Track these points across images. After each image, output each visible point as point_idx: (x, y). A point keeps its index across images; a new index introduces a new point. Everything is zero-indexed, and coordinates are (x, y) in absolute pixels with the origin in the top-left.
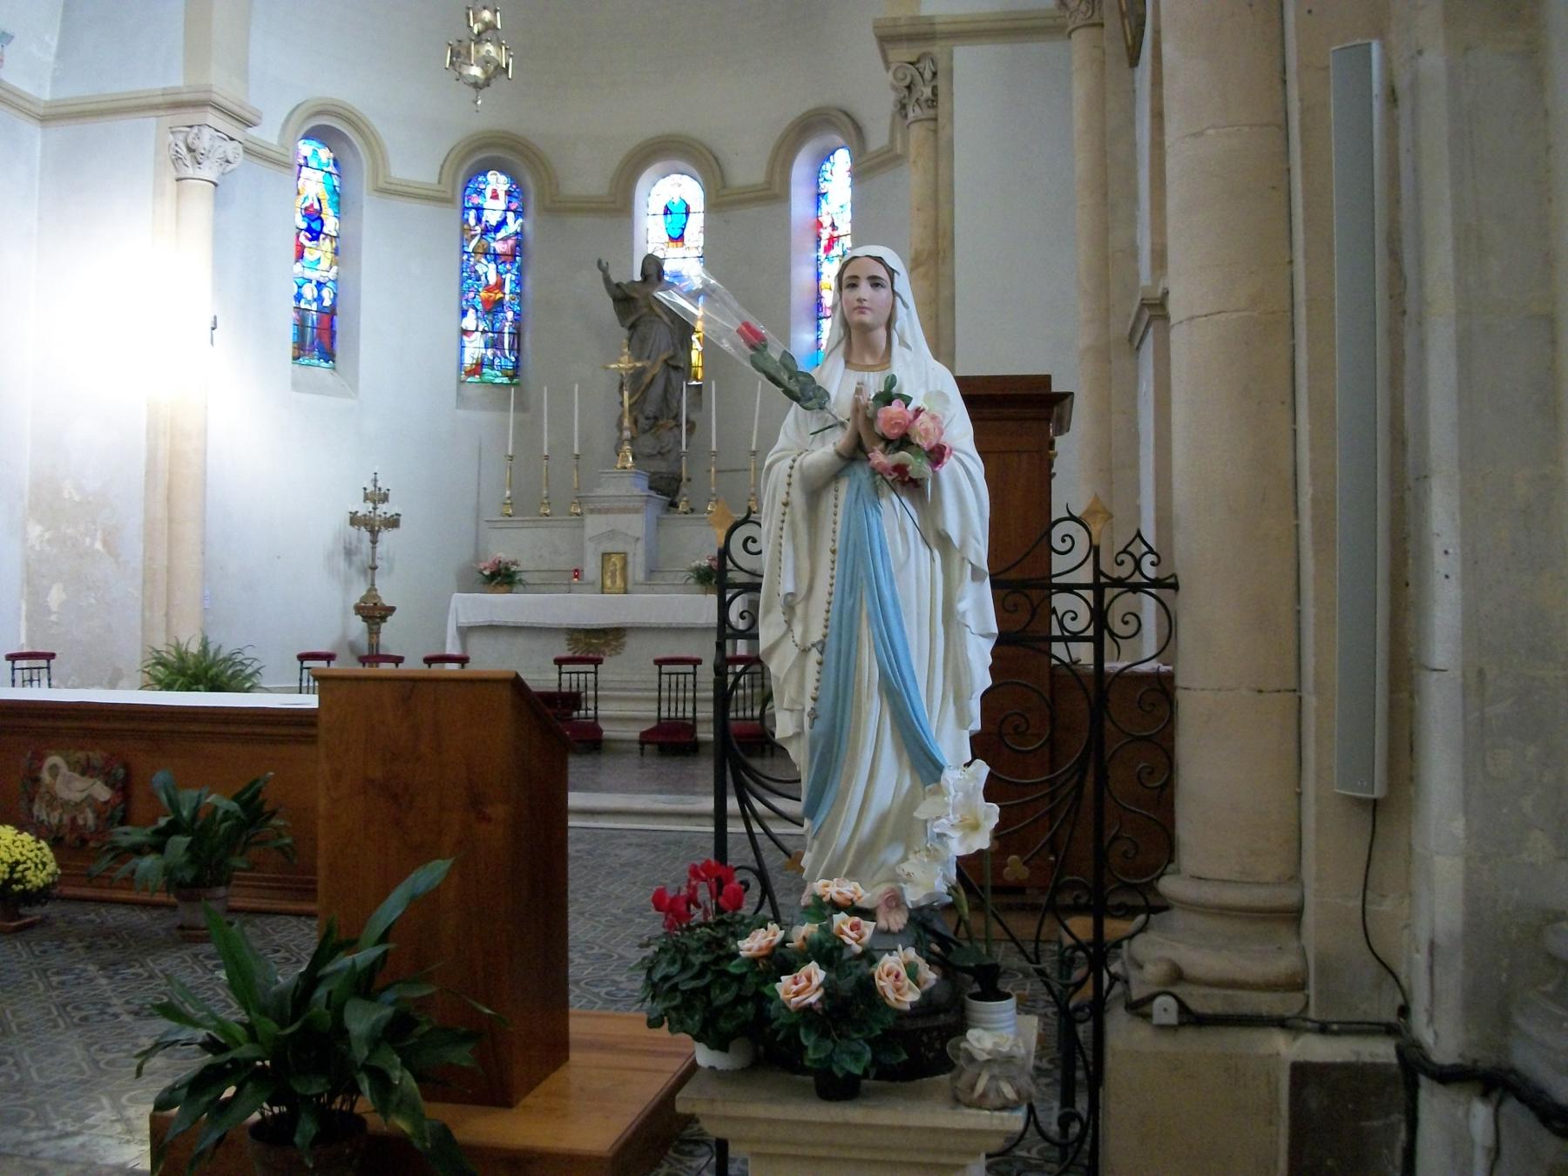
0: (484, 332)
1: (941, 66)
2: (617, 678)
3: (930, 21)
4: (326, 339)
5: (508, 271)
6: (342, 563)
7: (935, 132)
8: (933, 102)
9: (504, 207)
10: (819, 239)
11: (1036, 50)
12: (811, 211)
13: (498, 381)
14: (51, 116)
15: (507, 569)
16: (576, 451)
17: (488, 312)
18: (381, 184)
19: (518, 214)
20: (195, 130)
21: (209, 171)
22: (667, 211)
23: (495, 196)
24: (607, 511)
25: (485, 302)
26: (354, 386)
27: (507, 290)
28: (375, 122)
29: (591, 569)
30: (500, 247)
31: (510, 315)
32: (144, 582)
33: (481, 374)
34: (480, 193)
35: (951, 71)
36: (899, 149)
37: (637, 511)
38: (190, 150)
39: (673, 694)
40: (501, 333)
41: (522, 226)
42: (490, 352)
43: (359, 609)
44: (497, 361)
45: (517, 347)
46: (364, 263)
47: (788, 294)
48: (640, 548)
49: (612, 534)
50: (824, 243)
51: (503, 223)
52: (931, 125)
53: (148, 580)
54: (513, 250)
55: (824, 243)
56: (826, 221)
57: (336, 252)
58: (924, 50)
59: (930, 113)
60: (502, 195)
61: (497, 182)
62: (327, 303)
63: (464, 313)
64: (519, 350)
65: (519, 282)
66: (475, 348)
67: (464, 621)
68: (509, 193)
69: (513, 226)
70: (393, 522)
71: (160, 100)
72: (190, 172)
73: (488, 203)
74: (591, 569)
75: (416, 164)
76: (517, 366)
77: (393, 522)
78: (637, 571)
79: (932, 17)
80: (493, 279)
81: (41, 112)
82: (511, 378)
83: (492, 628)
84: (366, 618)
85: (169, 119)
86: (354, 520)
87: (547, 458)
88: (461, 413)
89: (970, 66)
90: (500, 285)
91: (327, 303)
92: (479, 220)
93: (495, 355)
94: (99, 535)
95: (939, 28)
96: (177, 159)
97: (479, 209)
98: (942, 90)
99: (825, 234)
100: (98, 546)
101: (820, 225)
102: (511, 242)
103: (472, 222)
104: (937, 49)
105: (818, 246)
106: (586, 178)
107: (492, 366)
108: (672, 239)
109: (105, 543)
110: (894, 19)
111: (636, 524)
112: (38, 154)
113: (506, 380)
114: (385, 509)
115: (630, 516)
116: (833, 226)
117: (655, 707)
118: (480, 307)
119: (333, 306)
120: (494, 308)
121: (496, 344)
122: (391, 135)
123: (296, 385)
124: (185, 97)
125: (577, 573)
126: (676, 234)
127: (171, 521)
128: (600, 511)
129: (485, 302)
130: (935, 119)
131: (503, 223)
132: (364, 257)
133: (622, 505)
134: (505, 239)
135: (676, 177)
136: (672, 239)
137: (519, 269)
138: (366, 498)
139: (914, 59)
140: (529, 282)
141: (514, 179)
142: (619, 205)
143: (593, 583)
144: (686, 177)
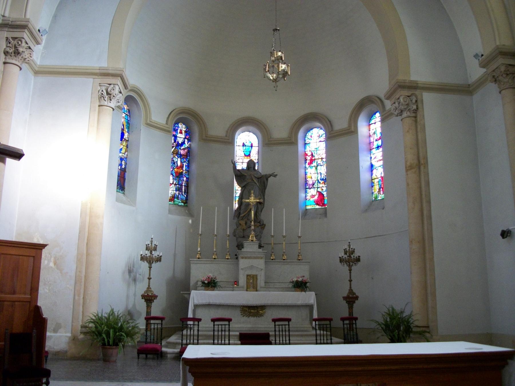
0: (175, 184)
1: (419, 97)
2: (263, 326)
3: (416, 82)
4: (122, 180)
5: (185, 162)
6: (127, 276)
7: (416, 121)
8: (416, 111)
9: (184, 137)
10: (306, 160)
11: (450, 97)
12: (303, 149)
13: (180, 204)
14: (39, 72)
15: (214, 281)
16: (200, 233)
17: (177, 177)
18: (148, 122)
19: (189, 140)
20: (112, 86)
21: (113, 104)
22: (244, 145)
23: (181, 133)
24: (249, 258)
25: (176, 173)
26: (132, 202)
27: (184, 169)
28: (147, 97)
29: (242, 281)
30: (182, 152)
31: (185, 179)
32: (75, 283)
33: (174, 201)
34: (176, 130)
35: (422, 101)
36: (353, 129)
37: (262, 258)
38: (108, 93)
39: (284, 333)
40: (182, 185)
41: (190, 145)
42: (177, 193)
43: (143, 297)
44: (180, 196)
45: (187, 192)
46: (140, 152)
47: (298, 177)
48: (263, 273)
49: (252, 267)
50: (308, 161)
51: (183, 143)
52: (414, 119)
53: (77, 281)
54: (187, 153)
55: (308, 161)
56: (309, 154)
57: (127, 147)
58: (412, 92)
59: (414, 115)
60: (183, 132)
61: (182, 127)
62: (123, 167)
64: (188, 193)
65: (188, 166)
66: (172, 190)
67: (196, 302)
68: (185, 132)
69: (186, 145)
70: (159, 259)
71: (98, 71)
72: (106, 103)
73: (179, 135)
74: (242, 281)
75: (159, 116)
76: (187, 199)
77: (159, 259)
78: (261, 282)
79: (417, 81)
80: (179, 164)
81: (37, 69)
82: (185, 203)
83: (209, 306)
84: (146, 300)
85: (99, 80)
86: (143, 258)
87: (216, 236)
88: (169, 215)
89: (428, 99)
90: (182, 167)
91: (123, 167)
92: (175, 141)
93: (179, 194)
94: (52, 259)
95: (420, 85)
96: (101, 97)
97: (175, 137)
98: (420, 106)
99: (309, 158)
100: (52, 264)
101: (306, 155)
102: (186, 151)
104: (417, 92)
105: (306, 163)
106: (217, 130)
107: (178, 198)
108: (245, 155)
109: (55, 264)
110: (404, 80)
111: (260, 263)
112: (32, 87)
113: (182, 204)
114: (155, 254)
115: (259, 260)
116: (312, 155)
117: (315, 339)
118: (174, 175)
119: (125, 168)
120: (178, 176)
121: (179, 189)
122: (152, 104)
123: (117, 200)
124: (110, 72)
125: (236, 283)
126: (247, 154)
127: (88, 254)
128: (246, 258)
129: (176, 173)
130: (416, 117)
131: (183, 143)
132: (141, 148)
133: (255, 256)
135: (247, 133)
136: (245, 155)
137: (189, 161)
138: (147, 249)
139: (409, 95)
140: (194, 167)
141: (187, 127)
142: (229, 141)
143: (243, 287)
144: (251, 133)
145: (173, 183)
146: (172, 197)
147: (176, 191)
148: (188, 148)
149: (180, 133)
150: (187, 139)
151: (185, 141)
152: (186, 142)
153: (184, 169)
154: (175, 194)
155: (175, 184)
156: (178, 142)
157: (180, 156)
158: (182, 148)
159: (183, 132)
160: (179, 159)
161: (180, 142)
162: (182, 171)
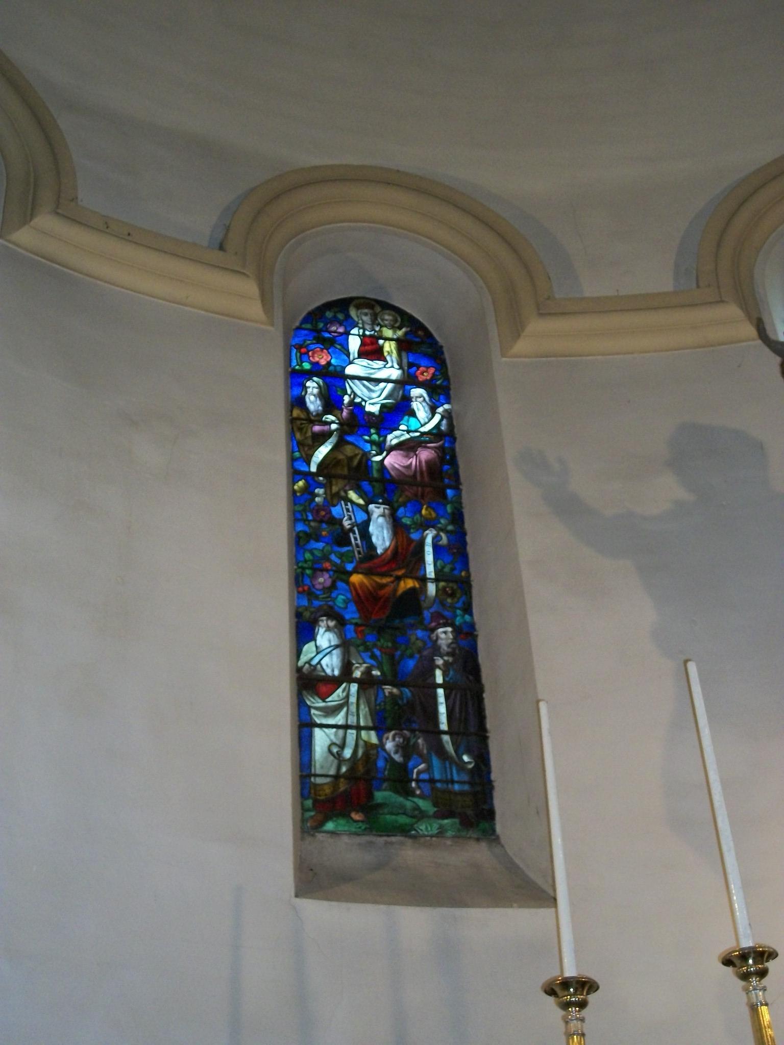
19: (439, 392)
23: (371, 351)
25: (366, 601)
31: (444, 635)
41: (447, 415)
51: (398, 409)
60: (389, 347)
63: (304, 631)
69: (423, 417)
80: (381, 536)
90: (406, 555)
92: (331, 401)
93: (406, 749)
102: (425, 455)
103: (313, 403)
118: (352, 614)
129: (366, 601)
131: (398, 409)
134: (408, 447)
145: (346, 674)
146: (351, 776)
147: (380, 727)
148: (436, 434)
149: (362, 354)
150: (428, 386)
151: (407, 399)
152: (420, 409)
153: (430, 571)
154: (371, 753)
155: (366, 683)
156: (357, 408)
157: (386, 487)
158: (393, 439)
159: (389, 347)
160: (377, 510)
161: (373, 408)
162: (410, 583)
